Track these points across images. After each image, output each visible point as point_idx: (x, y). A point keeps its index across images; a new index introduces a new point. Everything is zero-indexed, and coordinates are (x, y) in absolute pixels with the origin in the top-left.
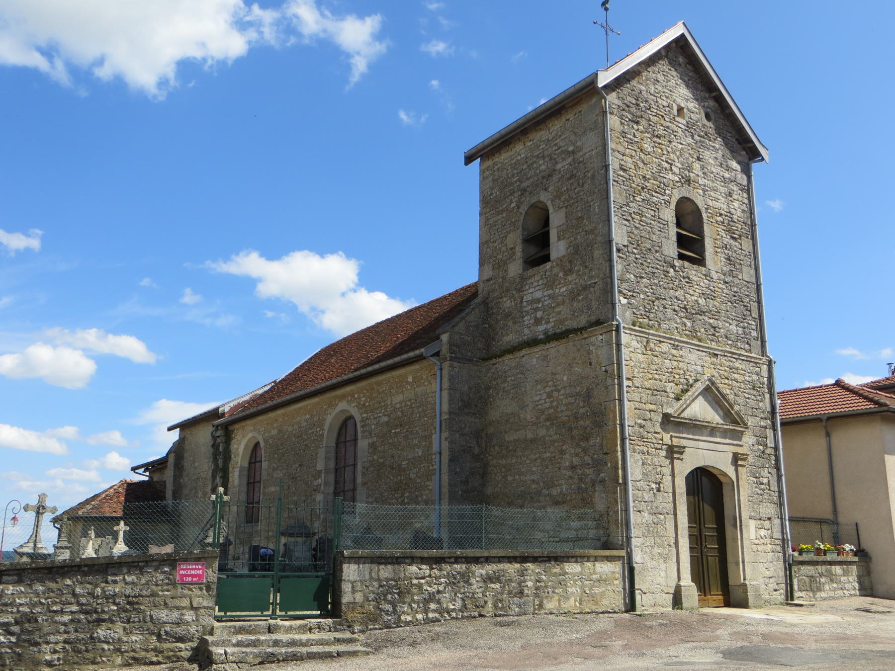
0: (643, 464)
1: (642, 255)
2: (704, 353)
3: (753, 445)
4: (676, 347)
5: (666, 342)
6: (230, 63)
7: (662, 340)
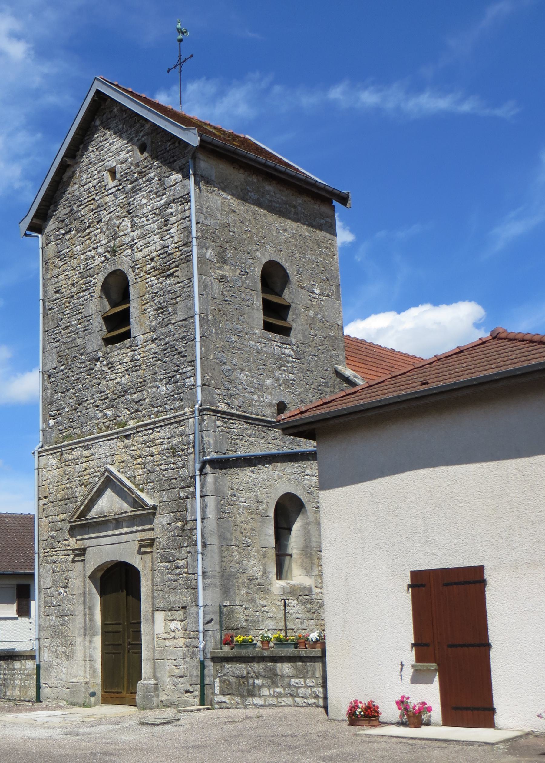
0: (53, 572)
1: (69, 368)
2: (115, 440)
3: (169, 524)
4: (86, 448)
5: (76, 448)
6: (204, 78)
7: (73, 447)
